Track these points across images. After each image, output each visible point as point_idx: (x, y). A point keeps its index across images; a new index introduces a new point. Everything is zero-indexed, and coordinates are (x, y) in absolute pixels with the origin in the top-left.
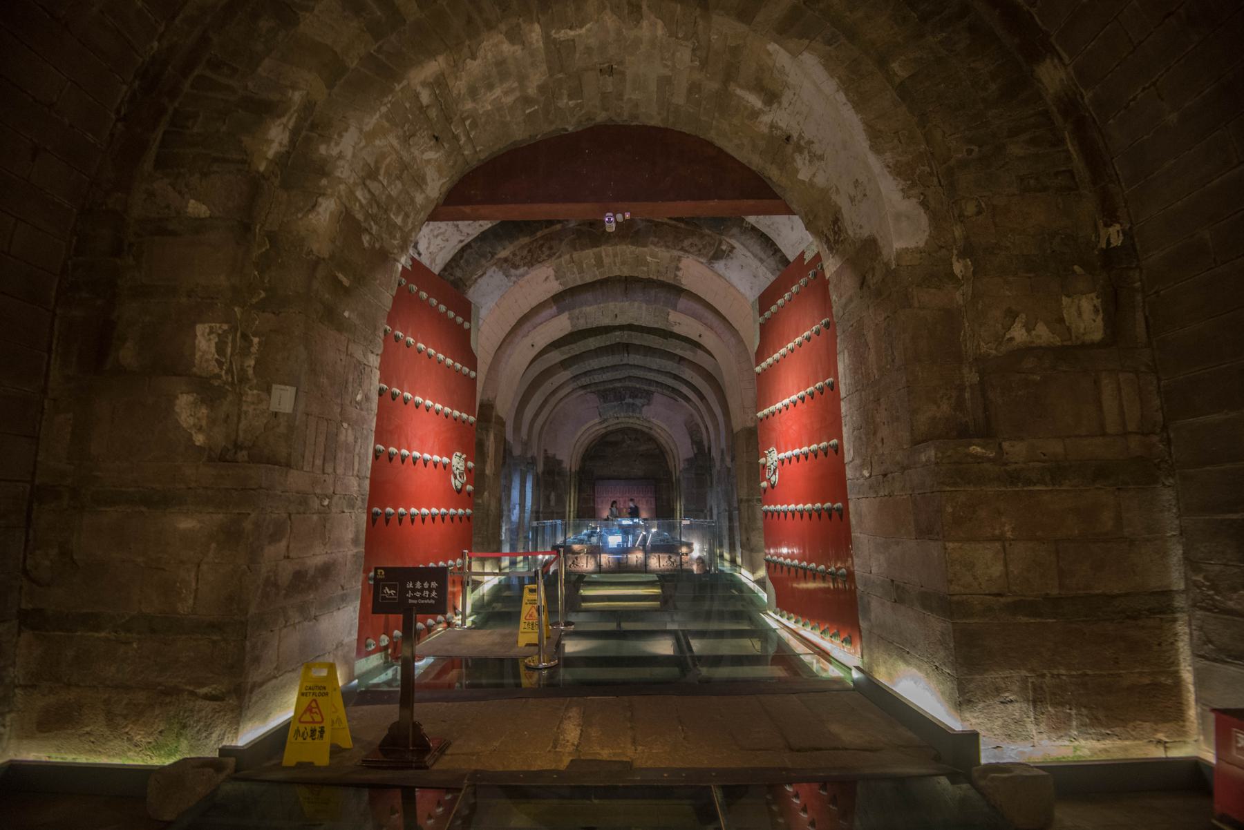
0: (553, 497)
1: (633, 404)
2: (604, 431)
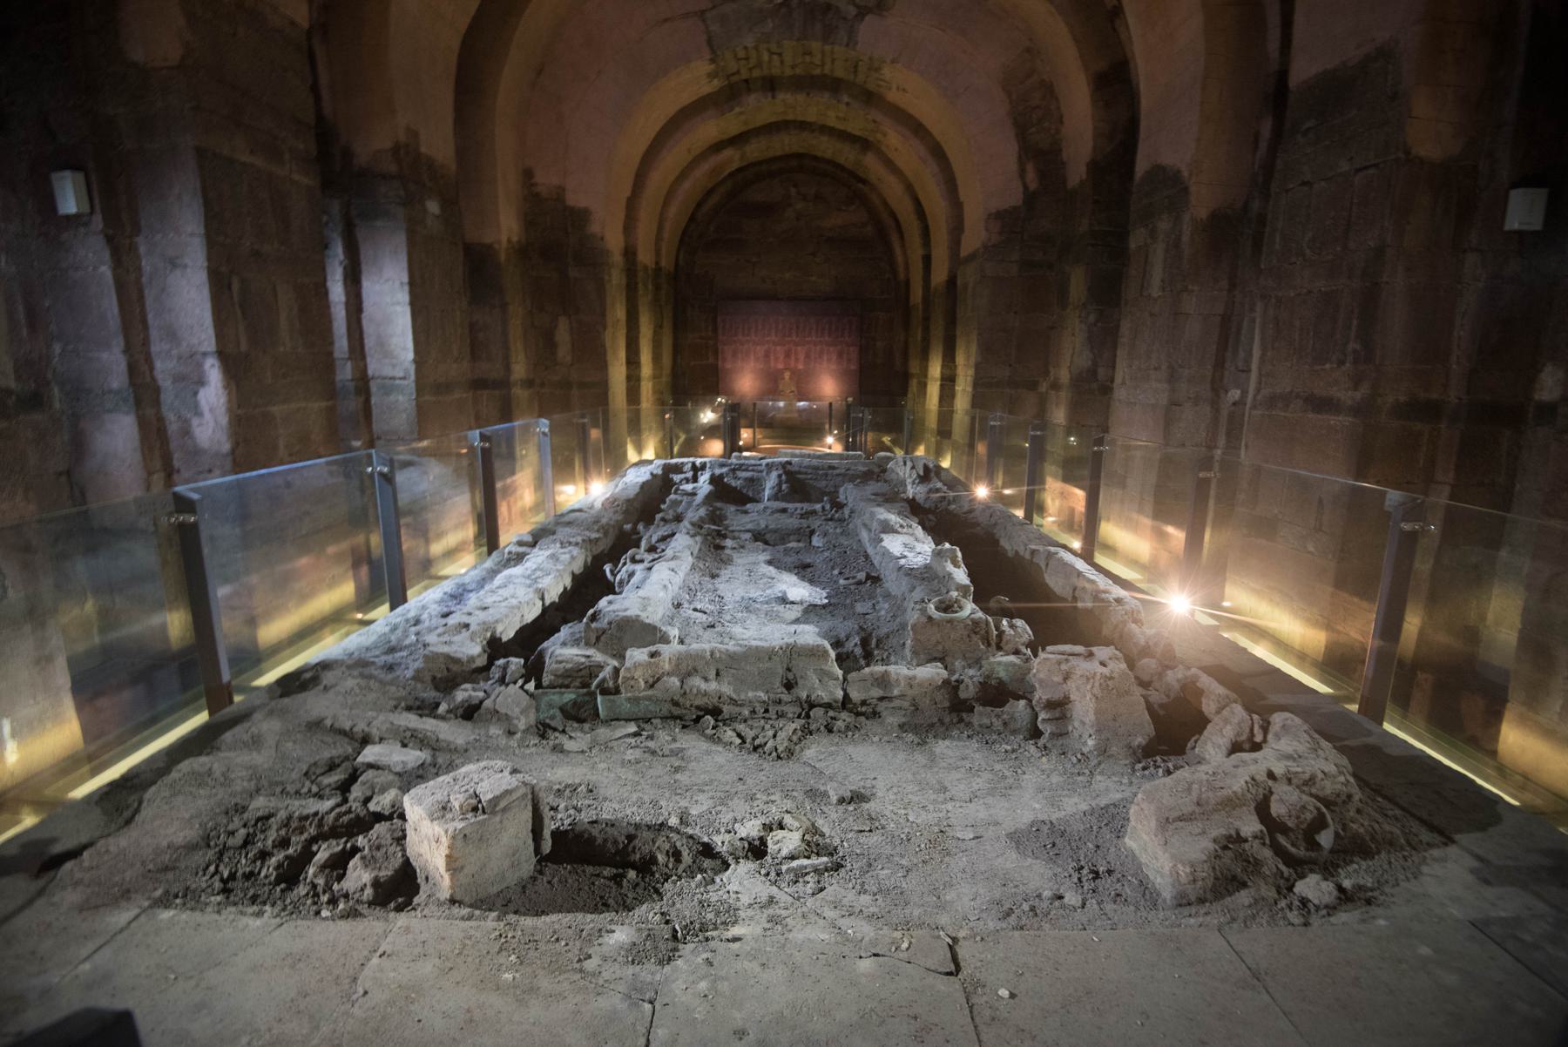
2: (732, 158)
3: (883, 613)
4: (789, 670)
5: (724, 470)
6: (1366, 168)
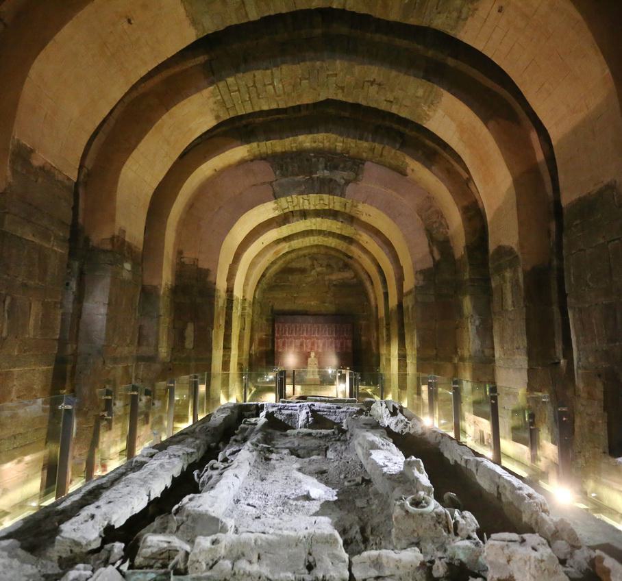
0: (190, 331)
1: (331, 180)
2: (285, 247)
3: (374, 507)
4: (310, 554)
5: (275, 409)
6: (614, 240)
